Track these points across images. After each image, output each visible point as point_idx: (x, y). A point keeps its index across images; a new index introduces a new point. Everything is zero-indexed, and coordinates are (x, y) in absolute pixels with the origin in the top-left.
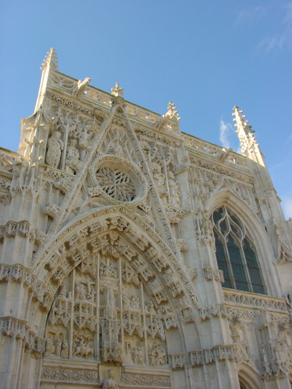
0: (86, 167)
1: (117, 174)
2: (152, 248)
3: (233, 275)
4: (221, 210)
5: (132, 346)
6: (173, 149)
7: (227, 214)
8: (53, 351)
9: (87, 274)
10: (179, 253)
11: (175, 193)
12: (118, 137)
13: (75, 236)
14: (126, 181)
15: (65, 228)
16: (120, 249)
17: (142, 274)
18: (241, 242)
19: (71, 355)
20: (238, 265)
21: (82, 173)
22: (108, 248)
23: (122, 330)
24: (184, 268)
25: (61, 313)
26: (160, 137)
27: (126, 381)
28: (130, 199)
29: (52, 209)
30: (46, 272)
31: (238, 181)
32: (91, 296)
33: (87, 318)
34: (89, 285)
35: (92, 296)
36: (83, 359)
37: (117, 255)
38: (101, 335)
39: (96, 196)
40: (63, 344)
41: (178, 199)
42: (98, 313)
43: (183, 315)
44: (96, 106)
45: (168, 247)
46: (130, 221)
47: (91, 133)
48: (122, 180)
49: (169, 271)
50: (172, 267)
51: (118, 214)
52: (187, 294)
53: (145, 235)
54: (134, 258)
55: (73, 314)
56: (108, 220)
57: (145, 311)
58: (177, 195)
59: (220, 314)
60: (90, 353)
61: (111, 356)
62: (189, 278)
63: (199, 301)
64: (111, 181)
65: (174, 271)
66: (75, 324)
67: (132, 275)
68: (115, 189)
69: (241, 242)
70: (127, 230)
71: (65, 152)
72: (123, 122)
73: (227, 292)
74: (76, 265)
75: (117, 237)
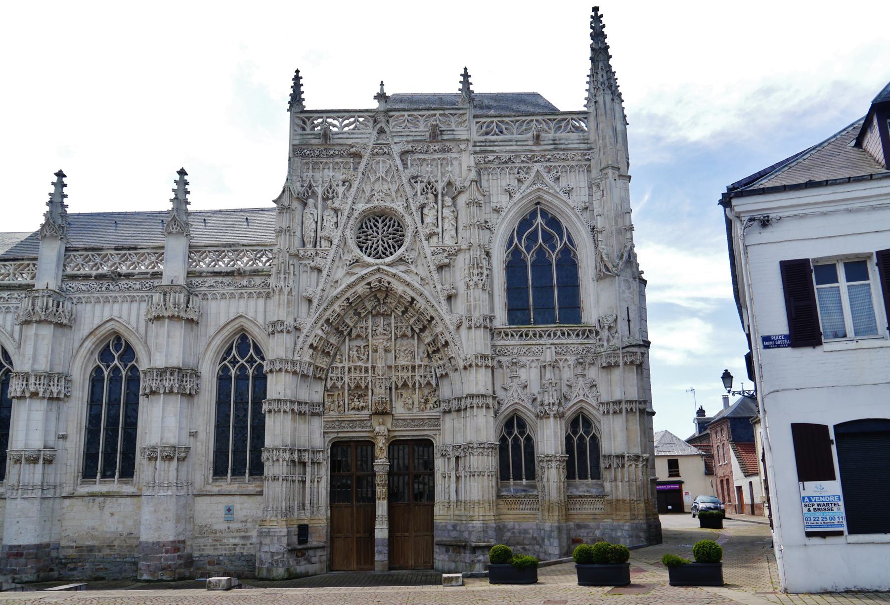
0: (339, 233)
1: (383, 222)
2: (415, 302)
3: (531, 304)
4: (533, 214)
5: (404, 396)
6: (458, 156)
7: (539, 219)
8: (332, 409)
9: (358, 336)
10: (444, 303)
11: (449, 226)
12: (381, 173)
13: (334, 311)
14: (393, 227)
15: (322, 308)
16: (391, 306)
17: (414, 327)
18: (554, 257)
19: (346, 410)
20: (543, 289)
21: (336, 241)
22: (377, 308)
23: (393, 383)
24: (447, 318)
25: (335, 378)
26: (436, 148)
27: (396, 426)
28: (397, 247)
29: (308, 295)
30: (311, 351)
31: (562, 164)
32: (363, 357)
33: (358, 378)
34: (362, 347)
35: (365, 358)
36: (357, 413)
37: (389, 312)
38: (373, 390)
39: (353, 263)
40: (339, 403)
41: (453, 233)
42: (370, 371)
43: (451, 362)
44: (350, 142)
45: (430, 298)
46: (390, 279)
47: (347, 184)
48: (389, 227)
49: (434, 322)
50: (437, 318)
51: (378, 276)
52: (451, 344)
53: (407, 289)
54: (404, 313)
55: (346, 377)
56: (369, 284)
57: (418, 362)
58: (451, 227)
59: (474, 364)
60: (363, 407)
61: (377, 409)
62: (452, 328)
63: (461, 349)
64: (375, 234)
65: (439, 321)
66: (348, 385)
67: (404, 329)
68: (380, 242)
69: (554, 257)
70: (389, 289)
71: (319, 223)
72: (386, 150)
73: (508, 330)
74: (345, 333)
75: (384, 295)
